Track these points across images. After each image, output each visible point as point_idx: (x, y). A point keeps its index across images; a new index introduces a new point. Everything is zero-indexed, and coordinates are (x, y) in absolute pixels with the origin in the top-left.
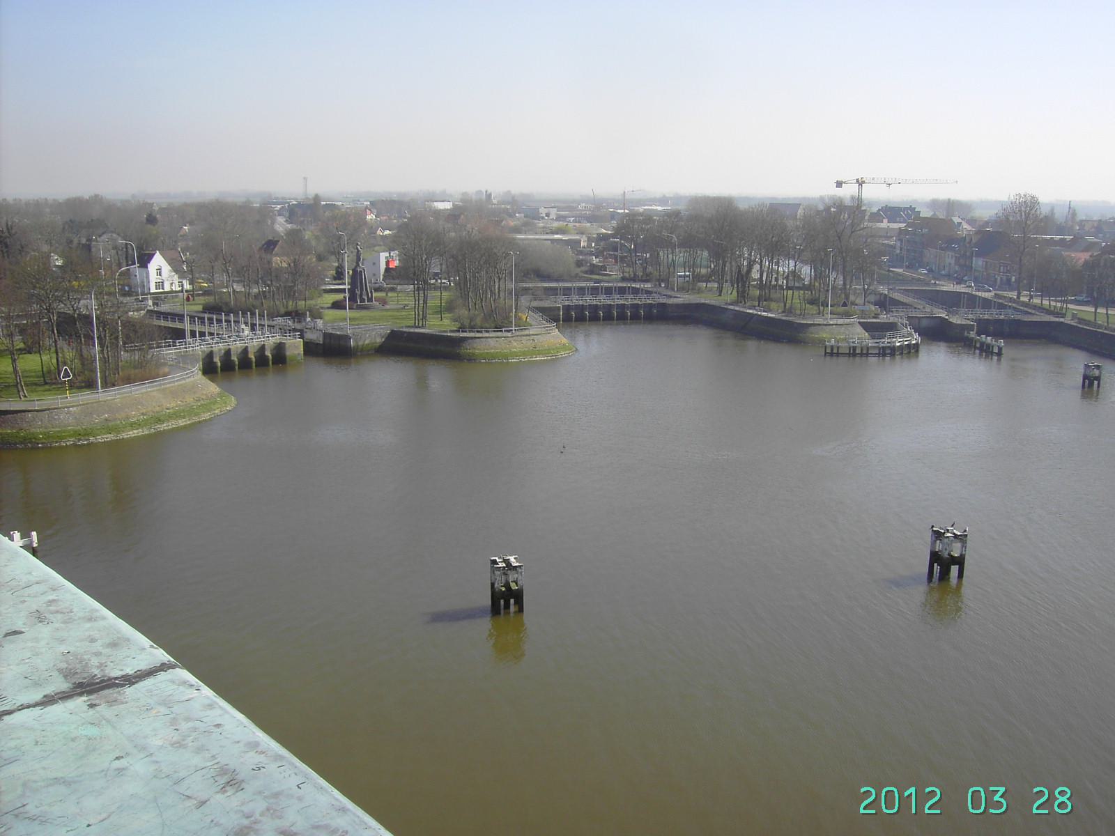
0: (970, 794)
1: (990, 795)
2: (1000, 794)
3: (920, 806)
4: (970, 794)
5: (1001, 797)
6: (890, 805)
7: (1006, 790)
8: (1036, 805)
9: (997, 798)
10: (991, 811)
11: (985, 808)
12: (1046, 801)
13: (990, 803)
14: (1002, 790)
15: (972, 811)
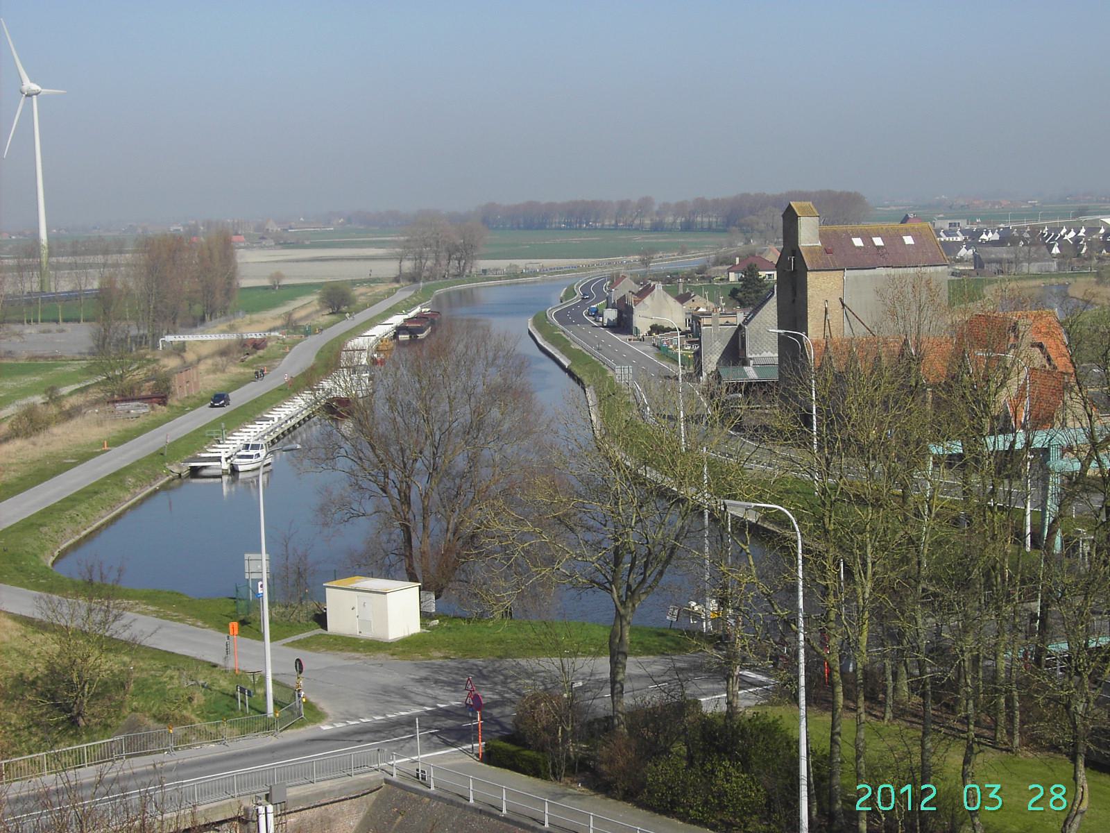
0: (965, 791)
1: (985, 792)
2: (995, 791)
3: (917, 801)
4: (965, 791)
5: (997, 794)
6: (886, 802)
7: (1001, 787)
8: (1031, 802)
9: (992, 795)
10: (987, 808)
11: (981, 805)
12: (1042, 797)
13: (986, 801)
14: (998, 787)
15: (967, 808)
